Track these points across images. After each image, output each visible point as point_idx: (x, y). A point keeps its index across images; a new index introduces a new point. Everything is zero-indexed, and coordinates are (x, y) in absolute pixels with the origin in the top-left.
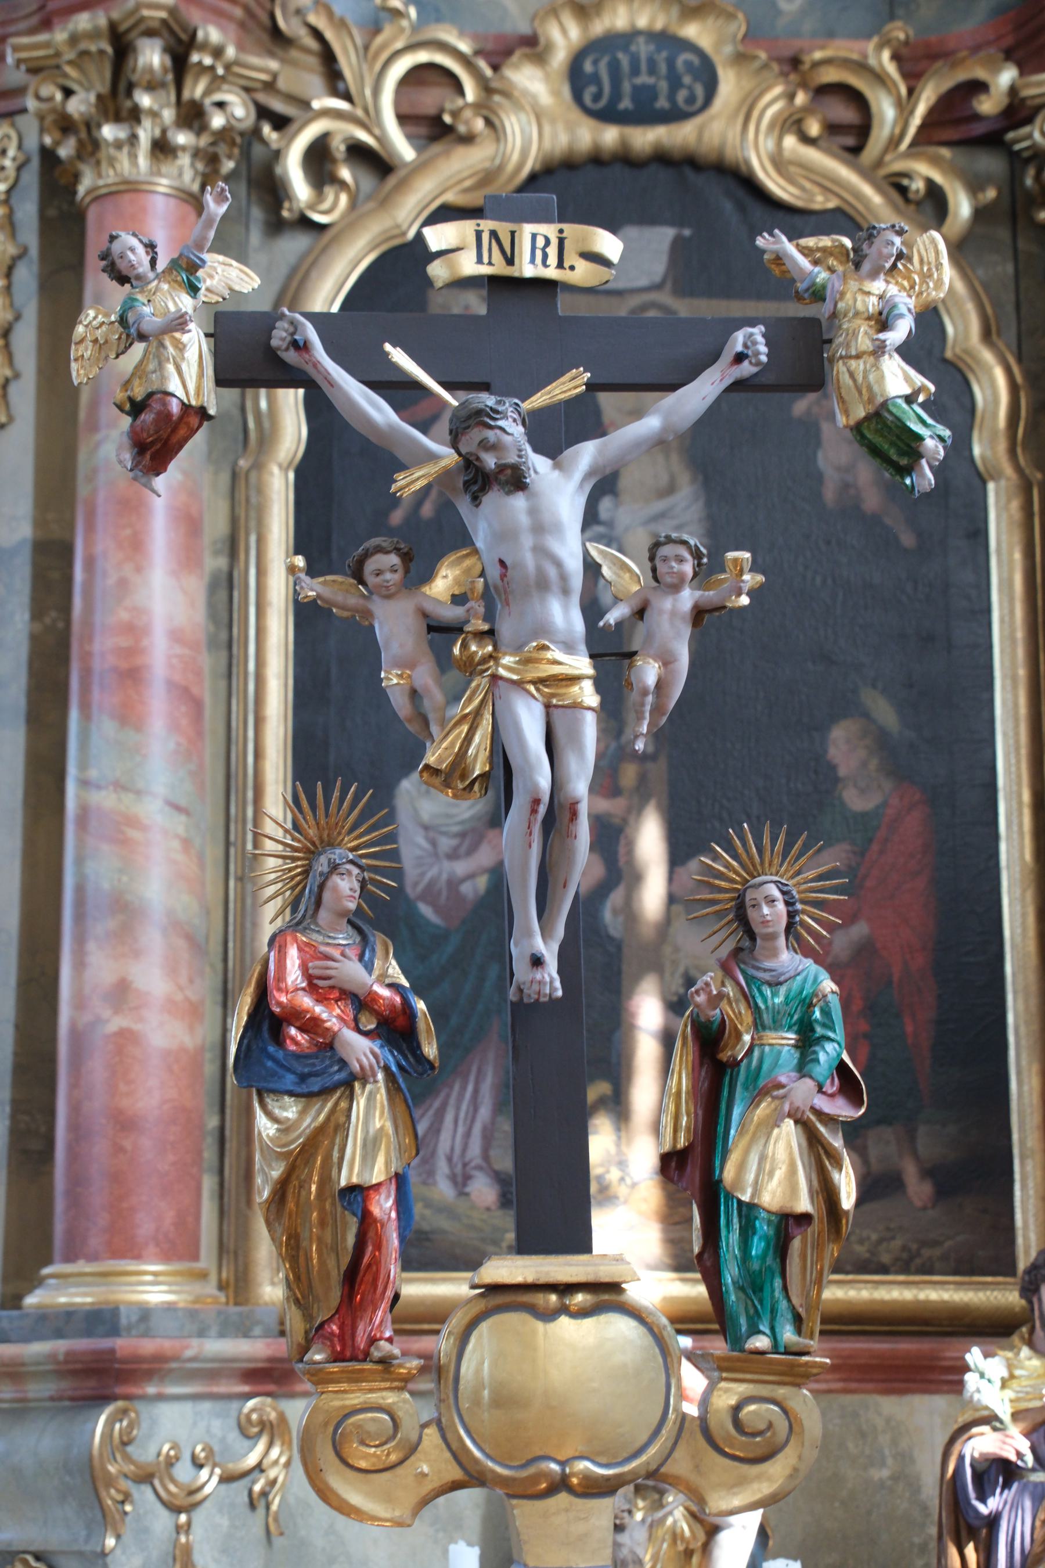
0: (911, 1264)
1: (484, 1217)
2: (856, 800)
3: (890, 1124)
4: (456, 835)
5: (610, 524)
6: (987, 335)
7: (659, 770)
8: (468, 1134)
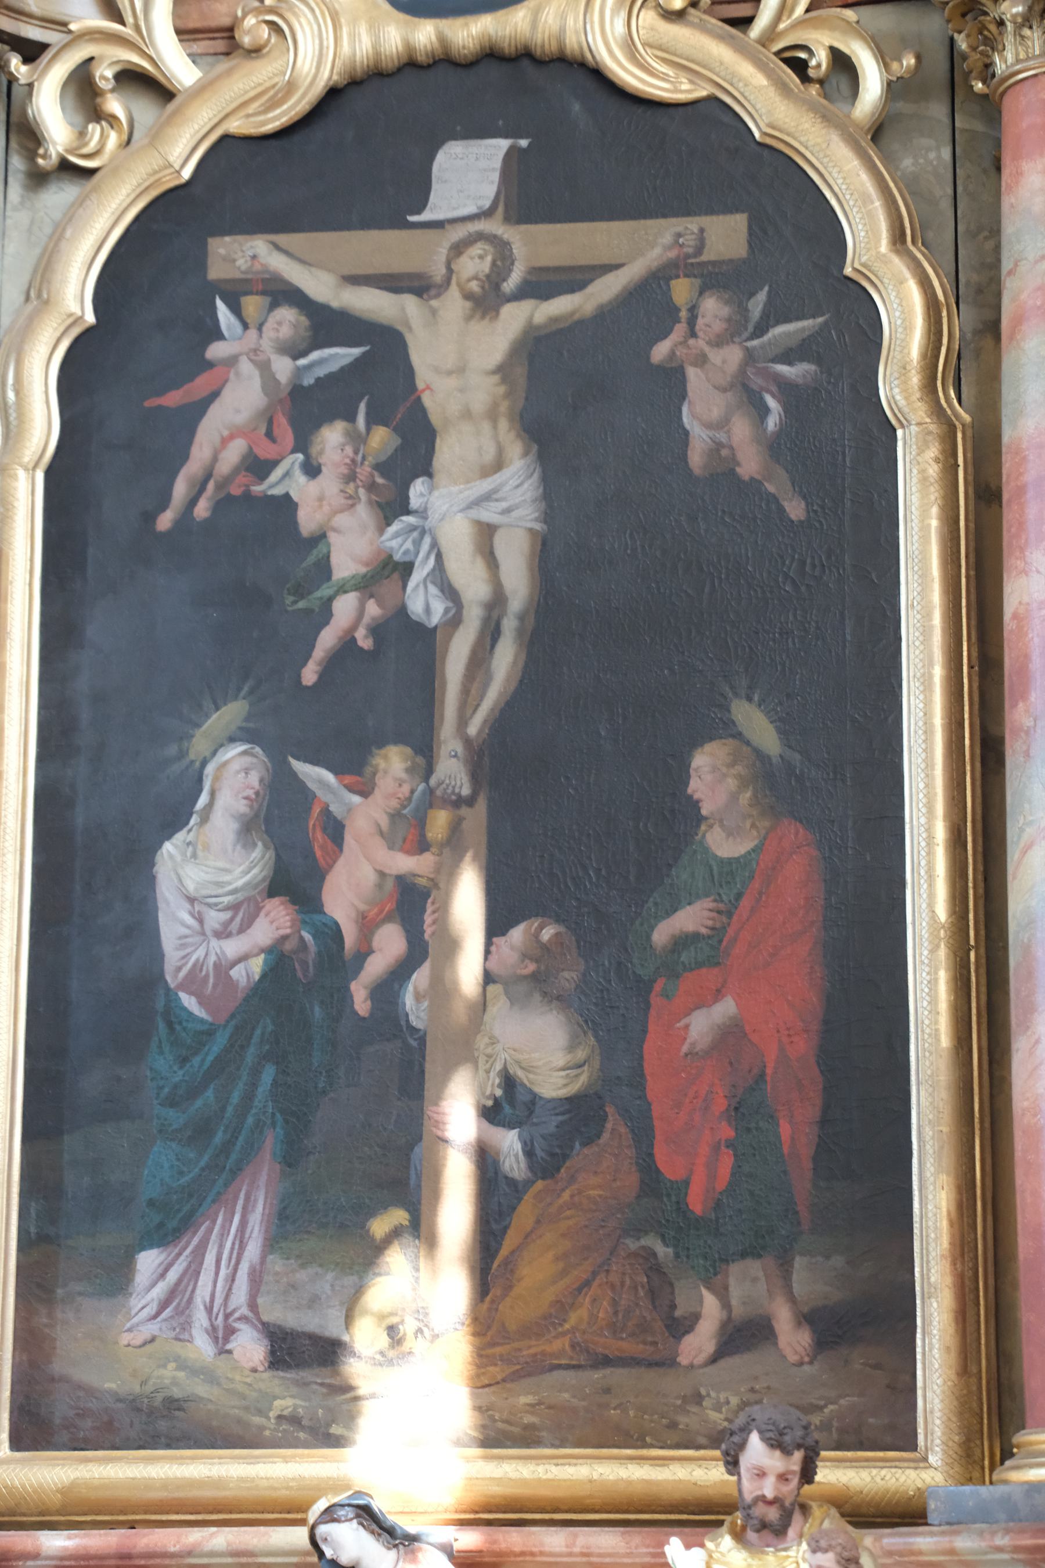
1: (248, 1380)
2: (724, 844)
3: (760, 1256)
5: (422, 513)
7: (477, 817)
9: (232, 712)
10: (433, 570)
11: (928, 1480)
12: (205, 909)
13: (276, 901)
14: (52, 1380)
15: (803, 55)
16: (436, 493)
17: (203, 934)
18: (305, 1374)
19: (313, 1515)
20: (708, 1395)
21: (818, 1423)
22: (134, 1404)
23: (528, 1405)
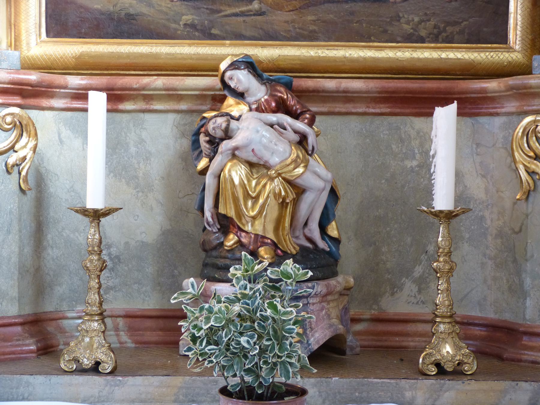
0: (439, 37)
1: (169, 6)
11: (514, 57)
19: (223, 66)
20: (404, 17)
21: (458, 30)
22: (110, 16)
23: (312, 20)
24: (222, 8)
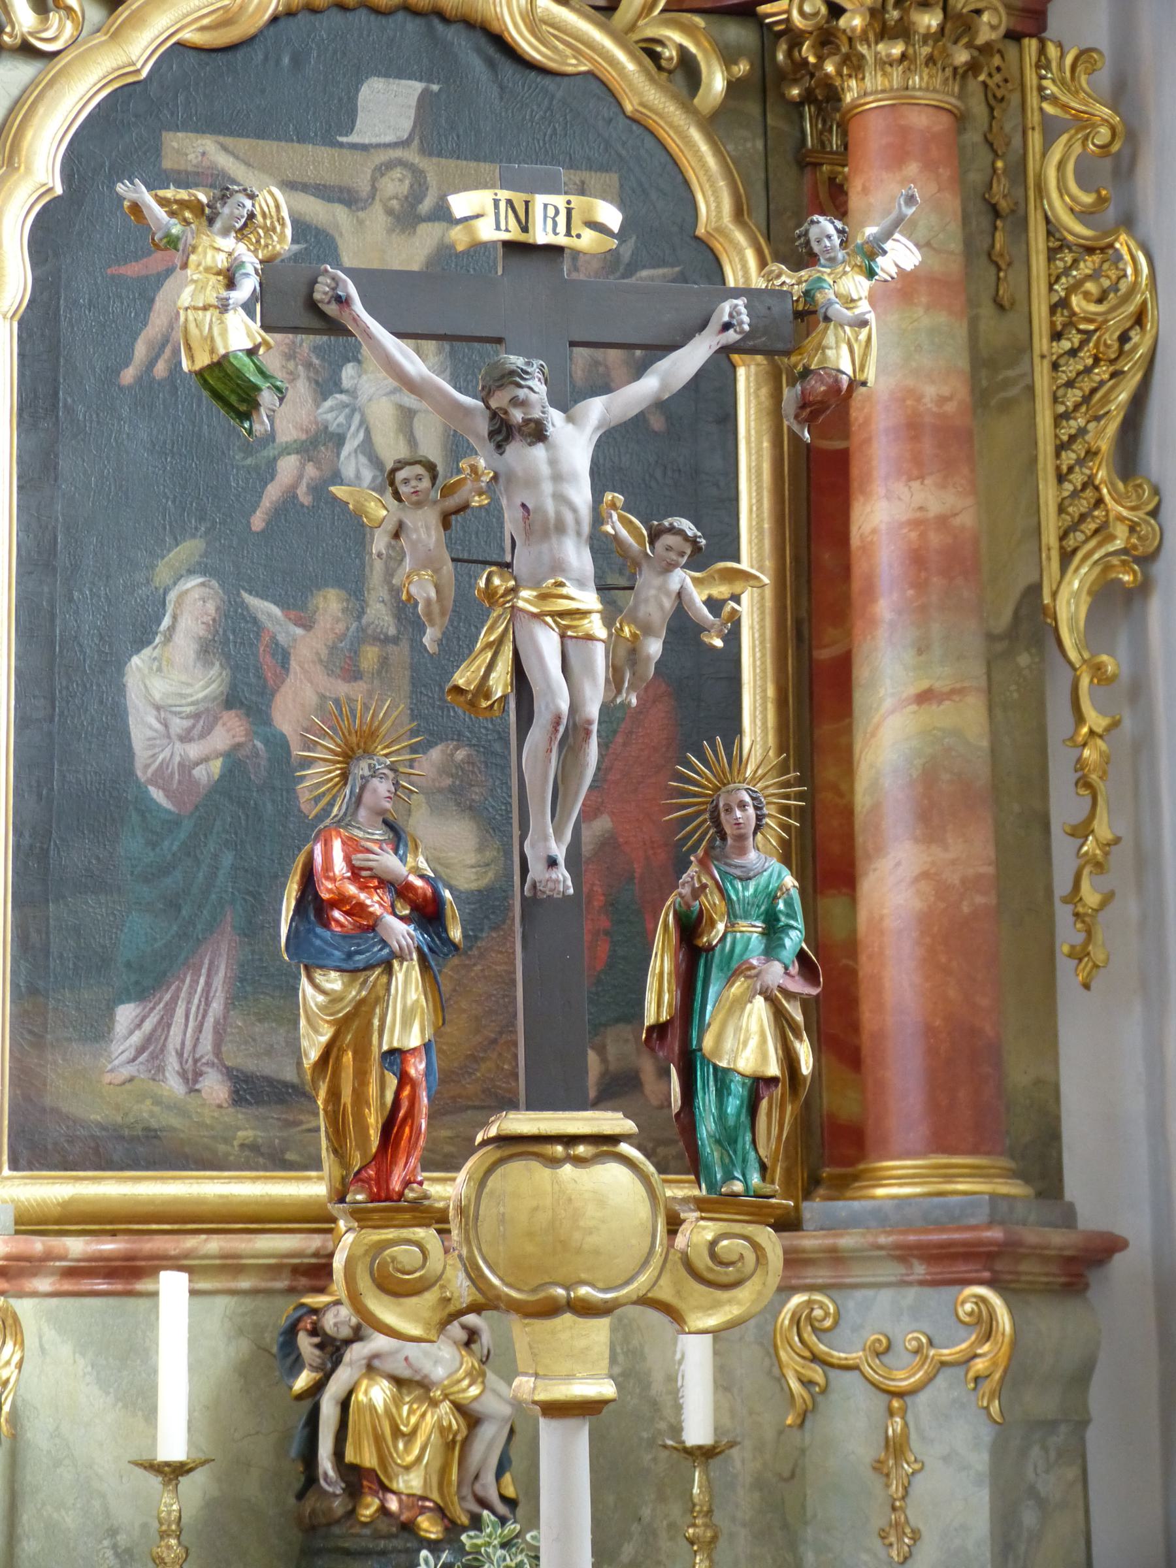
1: (216, 1114)
4: (188, 717)
5: (352, 393)
6: (739, 215)
8: (200, 1028)
9: (190, 548)
10: (363, 441)
12: (169, 716)
13: (232, 713)
14: (43, 1110)
15: (659, 49)
16: (364, 378)
17: (169, 737)
18: (263, 1110)
22: (116, 1134)
24: (302, 1117)
